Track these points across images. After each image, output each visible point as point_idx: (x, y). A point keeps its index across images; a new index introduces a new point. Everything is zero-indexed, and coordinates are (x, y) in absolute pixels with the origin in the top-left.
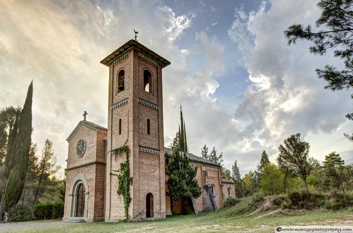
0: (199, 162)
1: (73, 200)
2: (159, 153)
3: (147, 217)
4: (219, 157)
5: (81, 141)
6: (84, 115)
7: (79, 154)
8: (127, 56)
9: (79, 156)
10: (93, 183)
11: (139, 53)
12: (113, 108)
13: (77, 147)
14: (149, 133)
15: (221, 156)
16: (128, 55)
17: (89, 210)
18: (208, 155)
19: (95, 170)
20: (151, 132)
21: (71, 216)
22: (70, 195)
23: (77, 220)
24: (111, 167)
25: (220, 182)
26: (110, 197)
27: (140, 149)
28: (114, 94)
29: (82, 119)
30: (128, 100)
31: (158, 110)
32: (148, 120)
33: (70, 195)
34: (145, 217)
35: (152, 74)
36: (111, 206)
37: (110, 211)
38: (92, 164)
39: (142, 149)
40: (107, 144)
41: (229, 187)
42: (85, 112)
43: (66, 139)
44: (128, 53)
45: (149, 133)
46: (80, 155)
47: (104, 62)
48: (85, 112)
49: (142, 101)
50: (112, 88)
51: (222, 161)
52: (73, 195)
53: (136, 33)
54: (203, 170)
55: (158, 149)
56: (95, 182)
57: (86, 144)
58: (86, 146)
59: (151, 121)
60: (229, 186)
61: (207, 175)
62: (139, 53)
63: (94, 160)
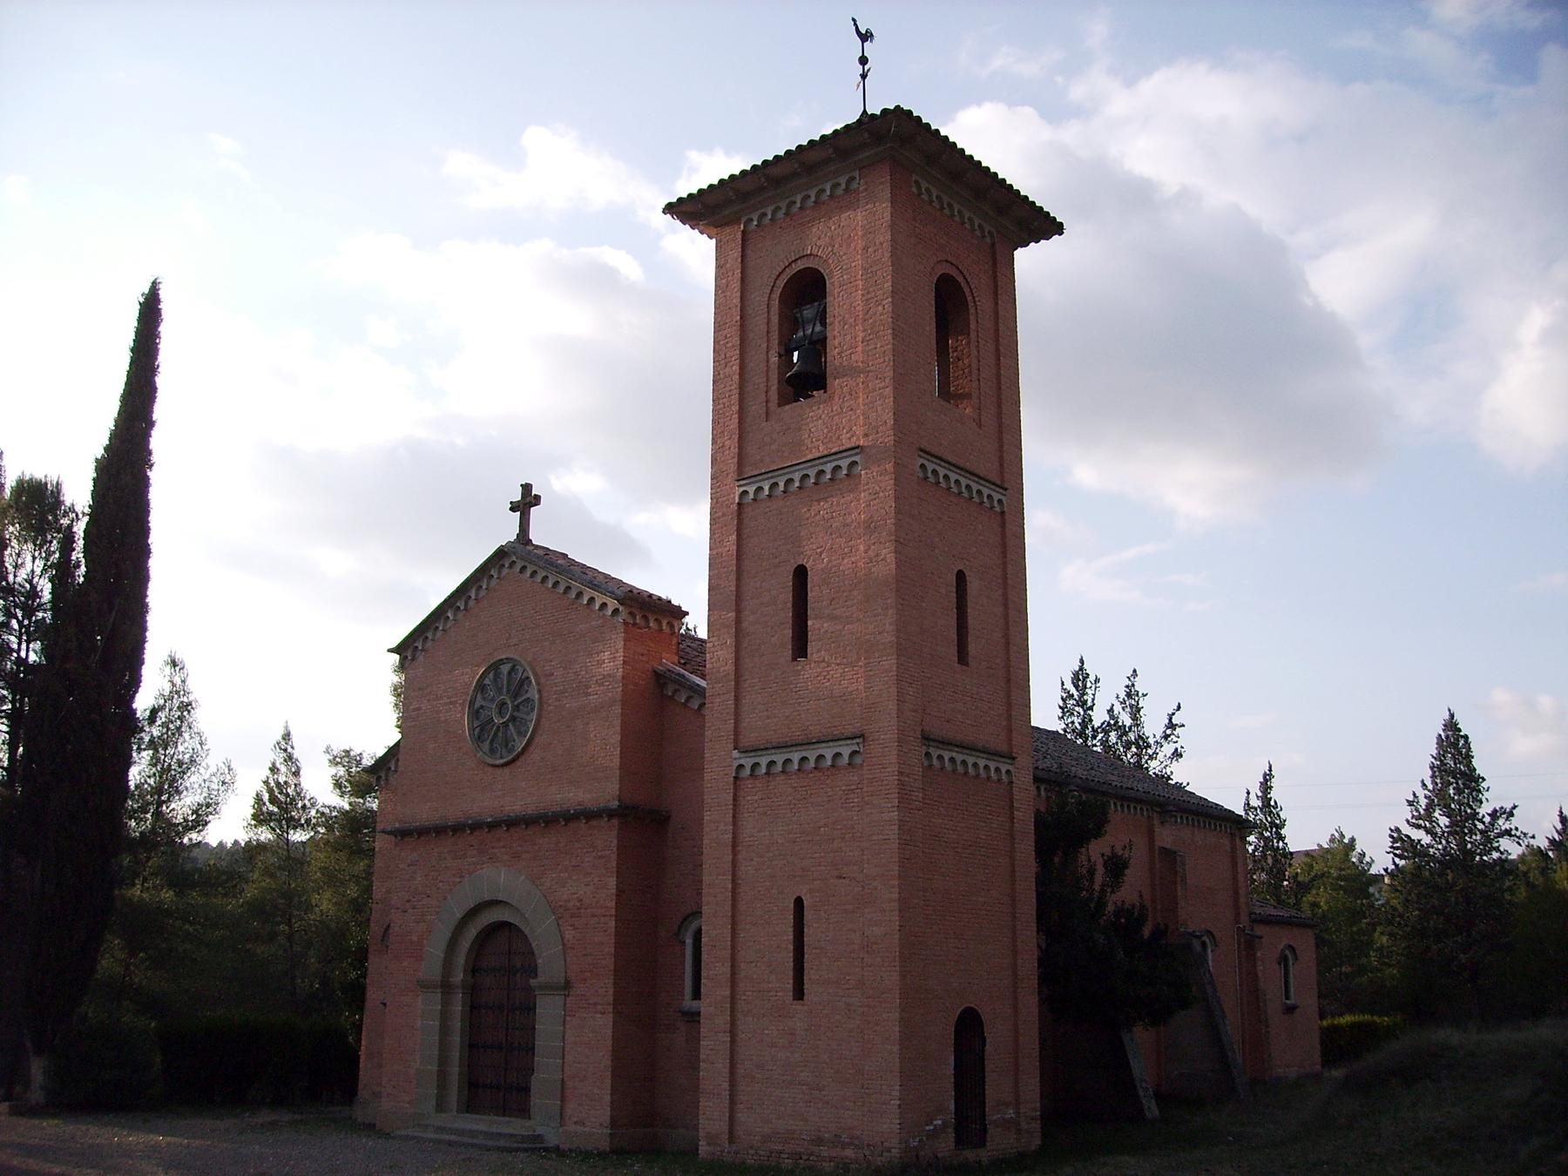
0: (1140, 801)
1: (445, 1016)
2: (1008, 772)
3: (960, 1141)
4: (1159, 734)
5: (505, 669)
6: (514, 507)
7: (486, 746)
8: (847, 190)
9: (490, 761)
10: (602, 937)
11: (914, 177)
12: (745, 493)
13: (472, 703)
14: (963, 656)
15: (1171, 726)
16: (854, 185)
17: (569, 1084)
18: (1097, 723)
19: (614, 857)
20: (973, 648)
21: (441, 1106)
22: (424, 986)
23: (500, 1134)
24: (734, 846)
25: (1244, 919)
26: (733, 1023)
27: (928, 755)
28: (756, 408)
29: (508, 530)
30: (856, 458)
31: (1003, 513)
32: (961, 576)
33: (424, 986)
34: (952, 1145)
35: (969, 298)
36: (740, 1071)
37: (733, 1102)
38: (589, 815)
39: (935, 753)
40: (706, 712)
41: (1291, 948)
42: (527, 488)
43: (394, 645)
44: (856, 174)
45: (963, 656)
46: (492, 751)
47: (684, 208)
48: (527, 488)
49: (957, 477)
50: (736, 368)
51: (1177, 755)
52: (446, 987)
53: (865, 37)
54: (1158, 844)
55: (1004, 748)
56: (613, 924)
57: (539, 691)
58: (540, 699)
59: (973, 586)
60: (1285, 942)
61: (1184, 880)
62: (914, 177)
63: (606, 792)
